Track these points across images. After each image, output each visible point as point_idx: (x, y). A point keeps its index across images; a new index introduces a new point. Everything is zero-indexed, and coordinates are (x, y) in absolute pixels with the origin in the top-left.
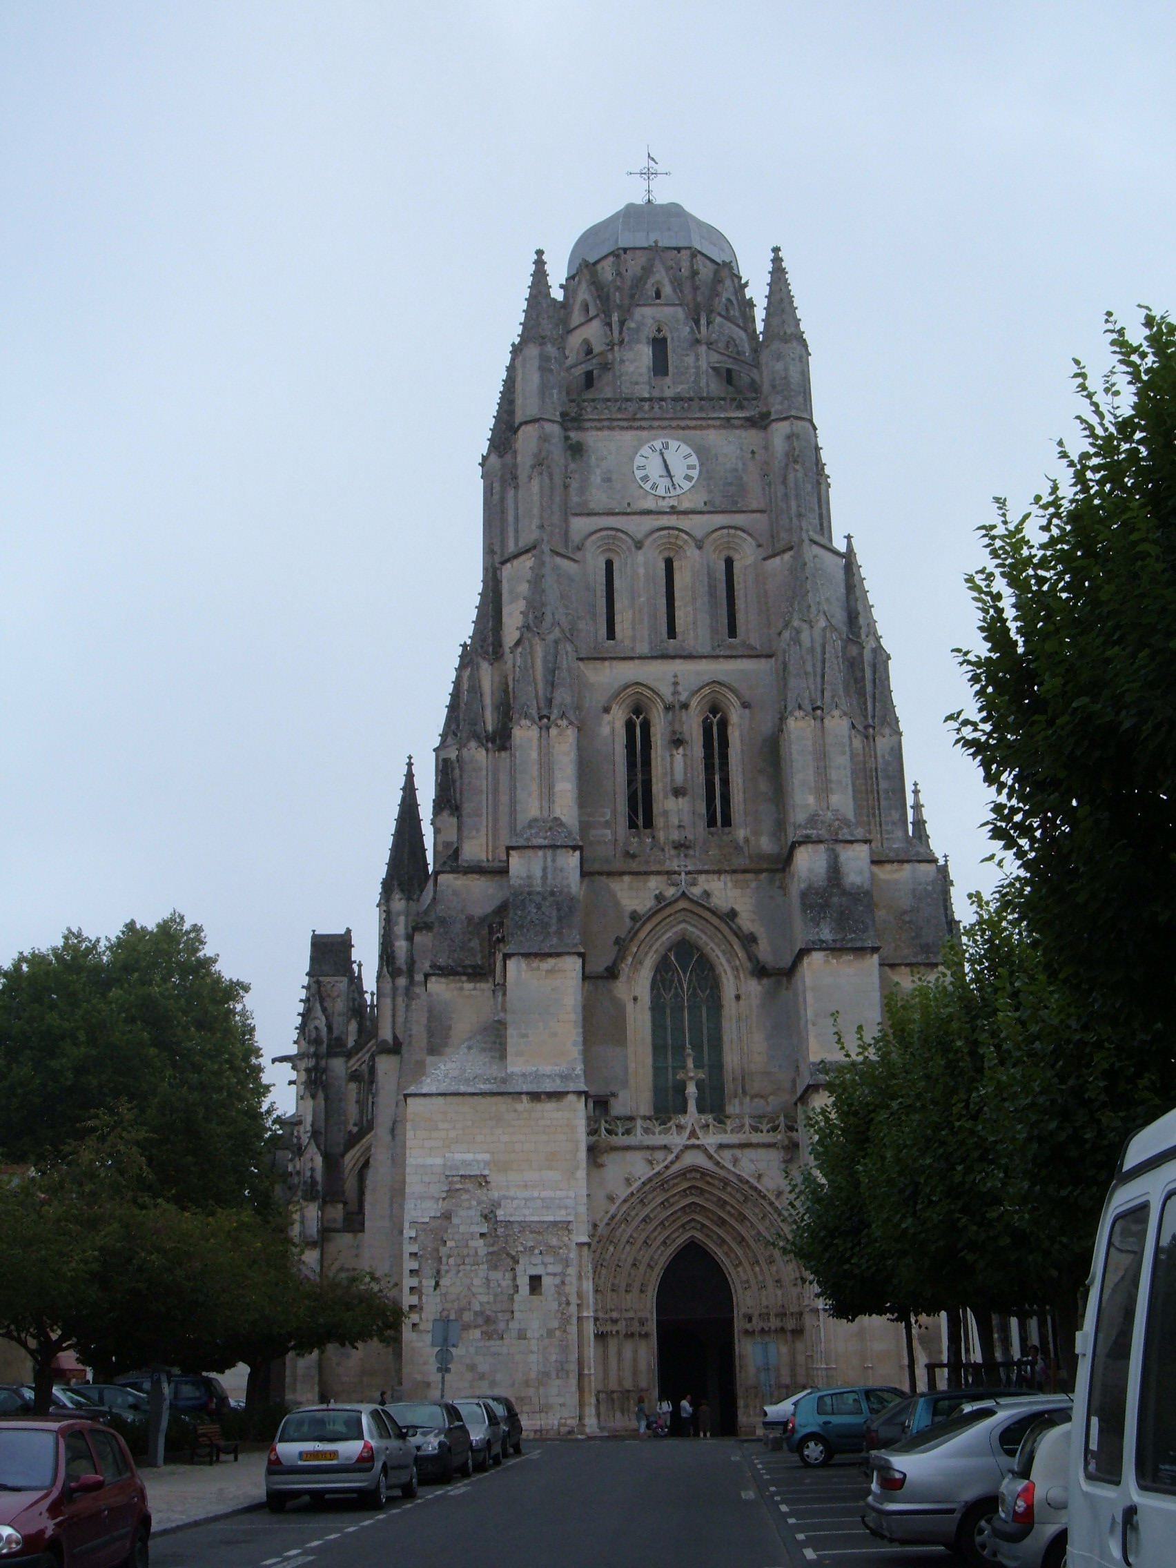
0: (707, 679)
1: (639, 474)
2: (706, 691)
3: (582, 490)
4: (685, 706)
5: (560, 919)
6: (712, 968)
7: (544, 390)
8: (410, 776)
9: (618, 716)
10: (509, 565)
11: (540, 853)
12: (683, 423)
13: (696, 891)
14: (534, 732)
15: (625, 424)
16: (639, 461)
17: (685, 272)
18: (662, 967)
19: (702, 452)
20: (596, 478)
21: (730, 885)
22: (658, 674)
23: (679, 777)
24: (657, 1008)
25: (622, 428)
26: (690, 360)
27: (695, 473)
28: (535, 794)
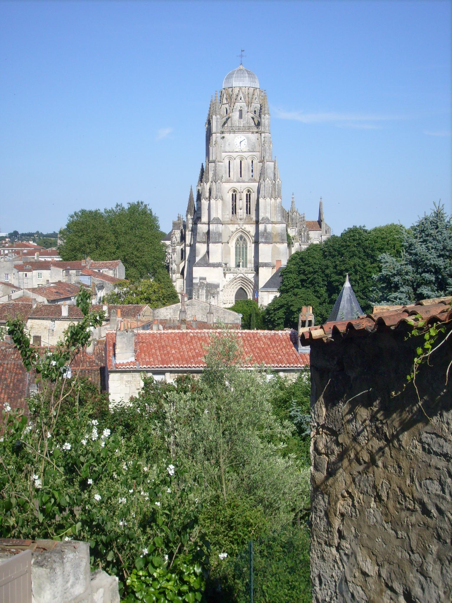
1: (235, 143)
3: (224, 147)
7: (217, 126)
8: (191, 189)
9: (231, 193)
13: (243, 227)
16: (235, 141)
17: (247, 93)
18: (238, 240)
19: (248, 138)
22: (238, 186)
24: (236, 248)
26: (247, 116)
27: (246, 143)
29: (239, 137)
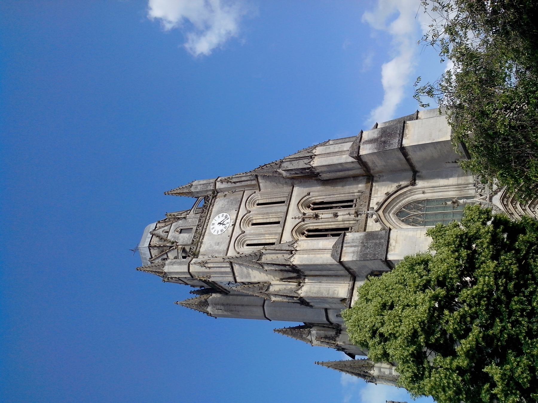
0: (296, 207)
1: (220, 233)
2: (300, 207)
4: (304, 214)
5: (374, 239)
6: (410, 204)
10: (237, 278)
11: (344, 249)
12: (208, 218)
13: (376, 207)
14: (296, 256)
15: (202, 237)
16: (215, 233)
19: (218, 213)
20: (216, 248)
21: (376, 196)
23: (331, 215)
25: (203, 239)
26: (190, 220)
27: (225, 214)
28: (322, 255)
29: (212, 227)
